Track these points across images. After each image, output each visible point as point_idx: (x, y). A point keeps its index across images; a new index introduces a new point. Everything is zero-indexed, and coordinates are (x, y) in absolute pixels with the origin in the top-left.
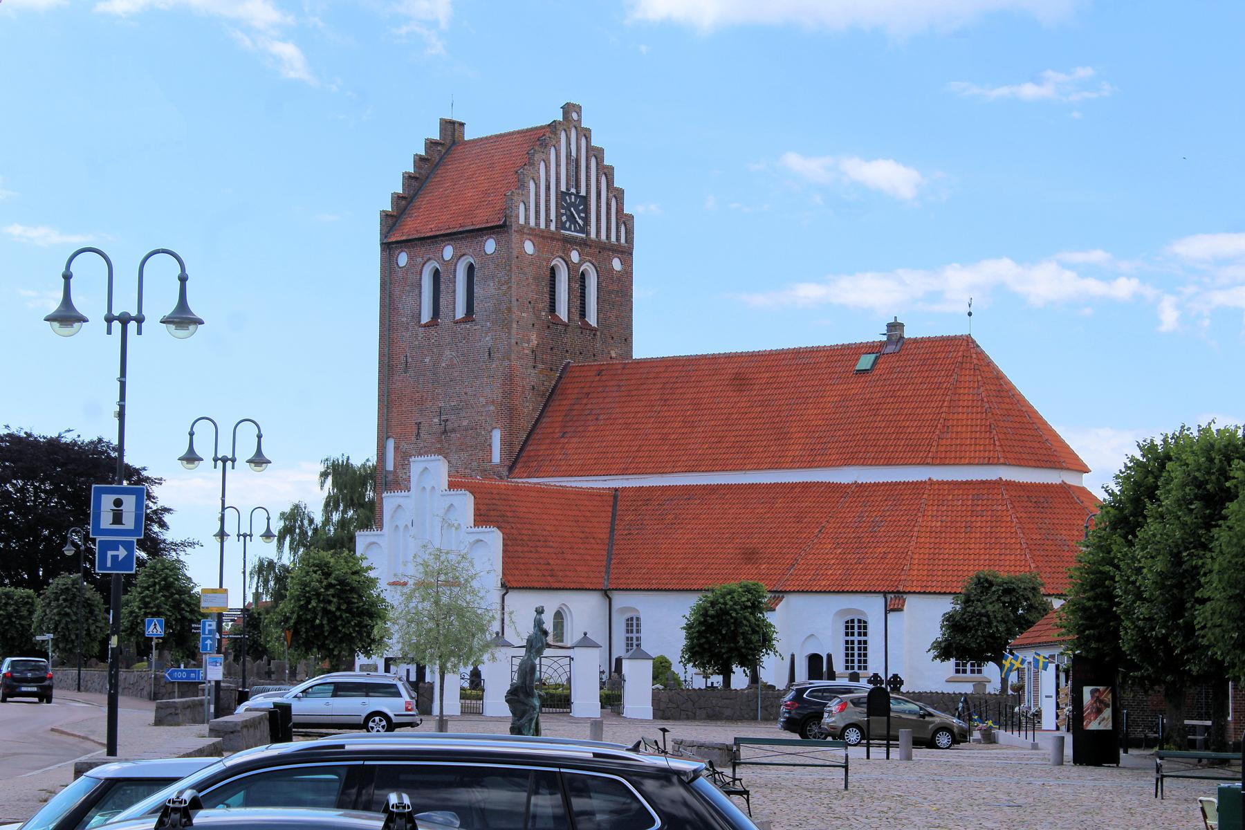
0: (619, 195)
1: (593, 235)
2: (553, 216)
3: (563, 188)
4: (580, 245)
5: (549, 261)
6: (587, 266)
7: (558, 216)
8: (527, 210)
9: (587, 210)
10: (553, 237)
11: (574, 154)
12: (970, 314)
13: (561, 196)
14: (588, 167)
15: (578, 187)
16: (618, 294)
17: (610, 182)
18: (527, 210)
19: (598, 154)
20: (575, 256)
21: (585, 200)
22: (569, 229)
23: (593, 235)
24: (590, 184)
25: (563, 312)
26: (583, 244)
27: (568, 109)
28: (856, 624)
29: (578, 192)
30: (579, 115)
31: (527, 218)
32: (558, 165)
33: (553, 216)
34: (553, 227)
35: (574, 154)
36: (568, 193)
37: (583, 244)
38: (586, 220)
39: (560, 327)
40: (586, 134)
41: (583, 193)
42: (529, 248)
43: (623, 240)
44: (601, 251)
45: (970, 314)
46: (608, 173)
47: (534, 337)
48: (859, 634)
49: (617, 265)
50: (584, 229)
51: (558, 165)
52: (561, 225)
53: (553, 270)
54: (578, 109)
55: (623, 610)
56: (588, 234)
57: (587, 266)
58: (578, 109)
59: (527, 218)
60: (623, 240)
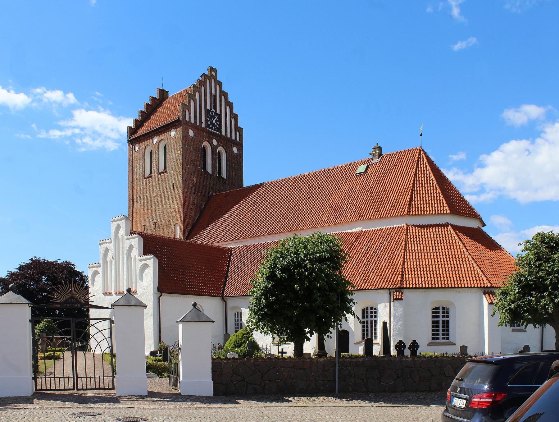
0: (236, 117)
1: (224, 134)
2: (203, 120)
3: (208, 108)
4: (217, 137)
5: (202, 142)
6: (220, 149)
7: (206, 121)
8: (190, 114)
9: (220, 120)
10: (203, 130)
11: (213, 92)
15: (216, 109)
16: (236, 163)
17: (236, 124)
18: (190, 114)
19: (226, 95)
20: (215, 142)
21: (220, 116)
23: (224, 134)
24: (221, 108)
25: (209, 170)
26: (219, 137)
28: (369, 311)
29: (216, 111)
30: (216, 74)
32: (205, 96)
33: (203, 120)
34: (203, 126)
35: (213, 92)
37: (219, 137)
38: (220, 125)
39: (208, 176)
40: (219, 84)
41: (218, 112)
44: (228, 143)
46: (231, 105)
47: (194, 179)
50: (219, 129)
51: (205, 96)
52: (207, 126)
53: (204, 149)
54: (215, 71)
55: (233, 308)
56: (221, 132)
57: (220, 149)
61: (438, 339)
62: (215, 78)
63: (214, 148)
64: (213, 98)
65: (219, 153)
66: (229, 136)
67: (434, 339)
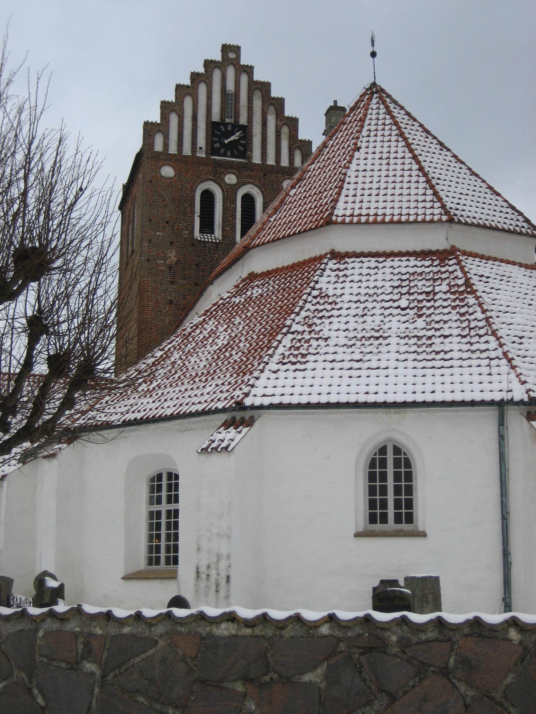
1: (257, 159)
2: (201, 142)
3: (216, 117)
7: (210, 142)
11: (230, 86)
12: (373, 54)
19: (264, 88)
21: (246, 130)
22: (225, 155)
27: (226, 49)
31: (166, 145)
35: (230, 86)
36: (222, 122)
40: (249, 70)
42: (168, 171)
45: (373, 54)
46: (279, 104)
52: (212, 150)
54: (237, 49)
56: (250, 158)
58: (237, 49)
59: (166, 145)
61: (158, 562)
62: (236, 63)
63: (229, 193)
64: (229, 100)
65: (248, 200)
66: (271, 161)
67: (150, 563)
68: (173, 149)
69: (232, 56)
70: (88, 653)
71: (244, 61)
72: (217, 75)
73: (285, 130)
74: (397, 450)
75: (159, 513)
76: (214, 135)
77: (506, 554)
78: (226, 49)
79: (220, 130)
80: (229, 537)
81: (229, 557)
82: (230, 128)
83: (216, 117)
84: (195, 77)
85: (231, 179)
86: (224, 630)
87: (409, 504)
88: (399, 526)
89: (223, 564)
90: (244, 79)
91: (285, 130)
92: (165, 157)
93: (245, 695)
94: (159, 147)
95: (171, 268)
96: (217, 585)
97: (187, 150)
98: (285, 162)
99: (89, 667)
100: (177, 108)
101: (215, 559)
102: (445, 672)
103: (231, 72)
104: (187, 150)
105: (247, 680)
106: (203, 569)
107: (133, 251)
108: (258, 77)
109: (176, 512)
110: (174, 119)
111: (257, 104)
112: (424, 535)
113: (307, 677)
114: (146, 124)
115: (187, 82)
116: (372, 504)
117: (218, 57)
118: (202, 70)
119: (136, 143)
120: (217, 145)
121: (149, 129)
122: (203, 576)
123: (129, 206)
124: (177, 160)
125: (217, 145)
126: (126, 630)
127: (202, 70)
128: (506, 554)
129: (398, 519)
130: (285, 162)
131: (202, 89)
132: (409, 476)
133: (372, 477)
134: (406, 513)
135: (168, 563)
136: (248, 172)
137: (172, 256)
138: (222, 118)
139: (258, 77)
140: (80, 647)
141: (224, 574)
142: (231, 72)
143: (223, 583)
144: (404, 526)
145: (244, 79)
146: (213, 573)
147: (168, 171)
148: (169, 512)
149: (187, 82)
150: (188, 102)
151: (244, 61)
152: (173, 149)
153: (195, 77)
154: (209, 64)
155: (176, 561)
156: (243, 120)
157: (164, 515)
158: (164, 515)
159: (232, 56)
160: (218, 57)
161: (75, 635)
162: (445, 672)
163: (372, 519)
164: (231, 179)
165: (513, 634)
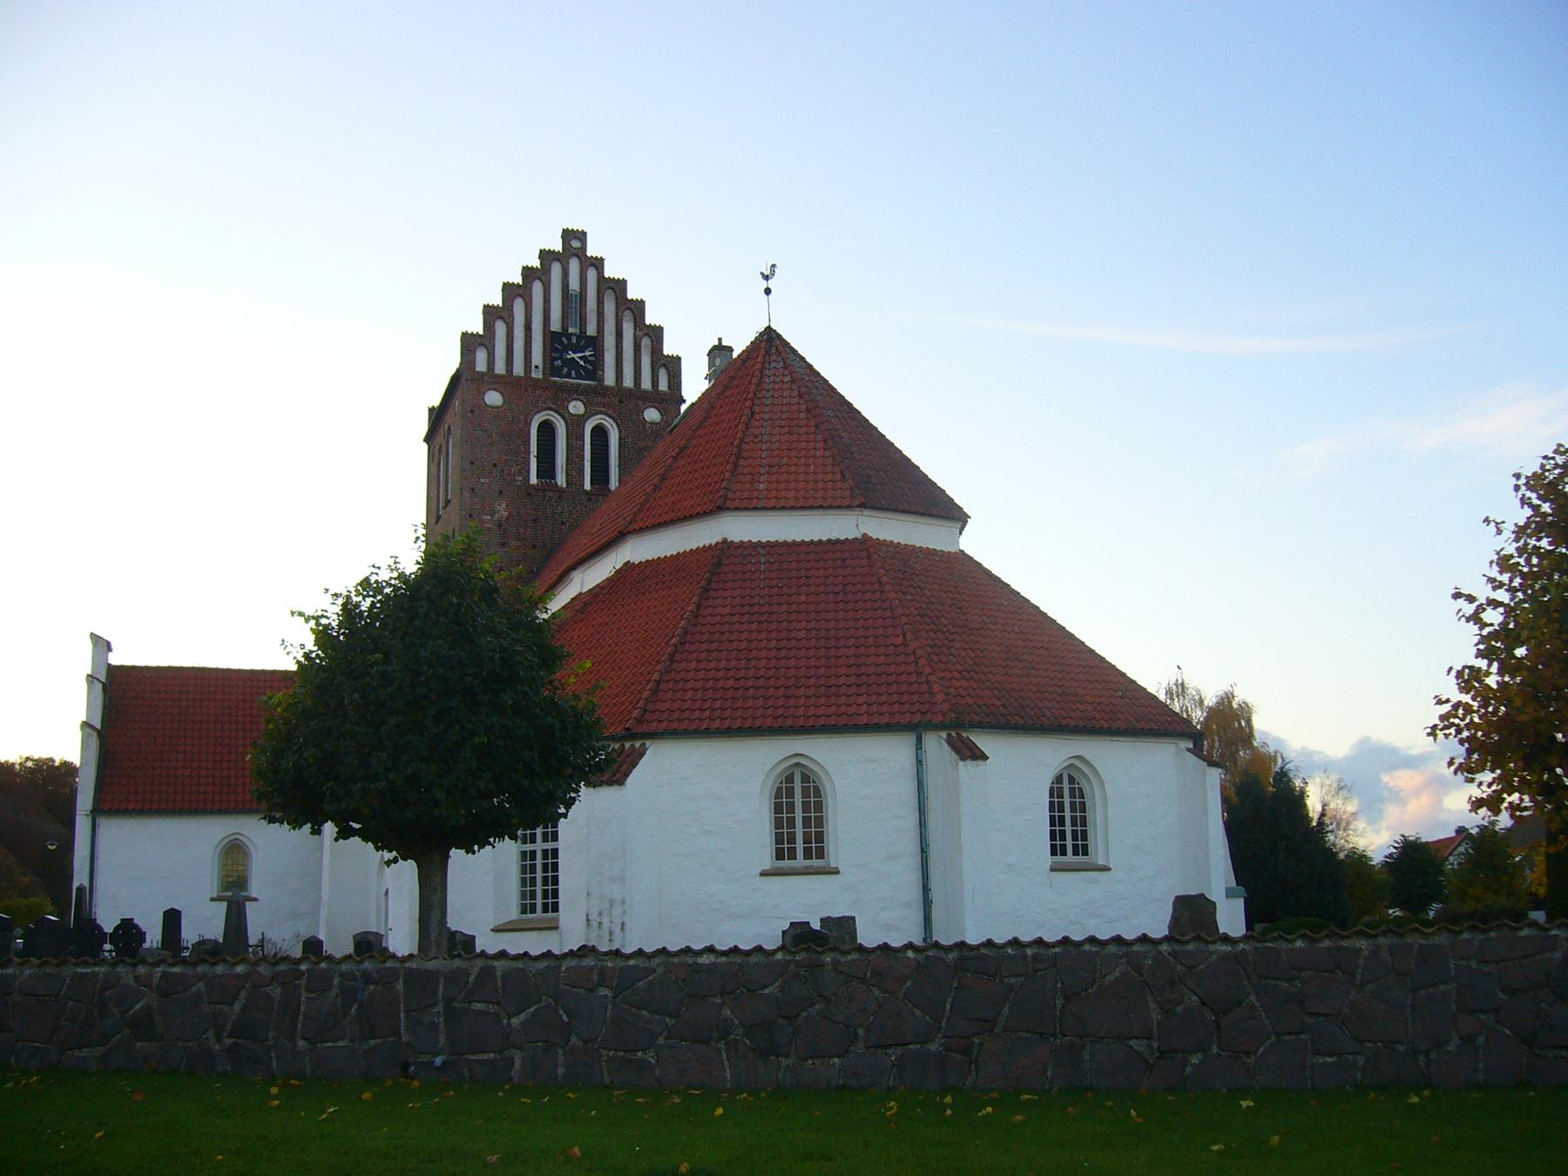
1: (609, 379)
2: (537, 358)
3: (556, 326)
11: (574, 284)
12: (768, 291)
13: (551, 339)
14: (600, 302)
19: (619, 286)
21: (596, 343)
24: (599, 318)
27: (567, 235)
34: (537, 375)
35: (574, 284)
40: (598, 263)
41: (591, 330)
42: (493, 398)
43: (663, 385)
45: (768, 291)
46: (638, 308)
48: (533, 853)
49: (652, 415)
52: (551, 368)
53: (547, 430)
54: (581, 236)
60: (663, 385)
61: (533, 911)
62: (581, 253)
63: (575, 425)
64: (573, 303)
65: (600, 434)
66: (628, 382)
67: (524, 912)
68: (500, 368)
69: (576, 244)
70: (602, 982)
71: (591, 251)
72: (556, 269)
73: (646, 342)
74: (805, 778)
75: (533, 853)
76: (554, 349)
77: (926, 889)
78: (567, 235)
79: (561, 343)
80: (623, 880)
81: (623, 902)
82: (574, 340)
83: (556, 326)
84: (527, 272)
85: (576, 407)
86: (705, 960)
87: (820, 838)
88: (809, 863)
89: (617, 911)
90: (592, 274)
91: (646, 342)
92: (490, 380)
93: (722, 1005)
94: (481, 366)
95: (500, 526)
96: (611, 934)
97: (519, 369)
98: (646, 384)
99: (603, 991)
100: (505, 315)
101: (607, 905)
102: (863, 980)
103: (574, 265)
104: (519, 369)
105: (723, 994)
106: (593, 917)
107: (447, 502)
108: (609, 272)
109: (555, 852)
110: (500, 328)
111: (610, 307)
112: (836, 872)
113: (766, 991)
114: (465, 336)
115: (517, 279)
116: (779, 839)
117: (557, 246)
118: (536, 263)
119: (453, 362)
120: (558, 363)
121: (469, 343)
122: (595, 924)
123: (439, 439)
124: (506, 383)
125: (558, 363)
126: (631, 962)
127: (536, 263)
128: (926, 889)
129: (808, 854)
130: (646, 384)
131: (537, 288)
132: (819, 806)
133: (778, 808)
134: (816, 846)
135: (545, 910)
136: (598, 397)
137: (502, 510)
138: (565, 328)
139: (609, 272)
140: (595, 977)
141: (618, 921)
142: (574, 265)
143: (617, 929)
144: (815, 862)
145: (592, 274)
146: (606, 920)
147: (493, 398)
148: (545, 852)
149: (517, 279)
150: (519, 306)
151: (591, 251)
152: (500, 368)
153: (527, 272)
154: (545, 255)
155: (555, 908)
156: (591, 330)
157: (539, 855)
158: (539, 855)
159: (576, 244)
160: (557, 246)
161: (591, 969)
162: (863, 980)
163: (779, 855)
164: (576, 407)
165: (910, 954)
